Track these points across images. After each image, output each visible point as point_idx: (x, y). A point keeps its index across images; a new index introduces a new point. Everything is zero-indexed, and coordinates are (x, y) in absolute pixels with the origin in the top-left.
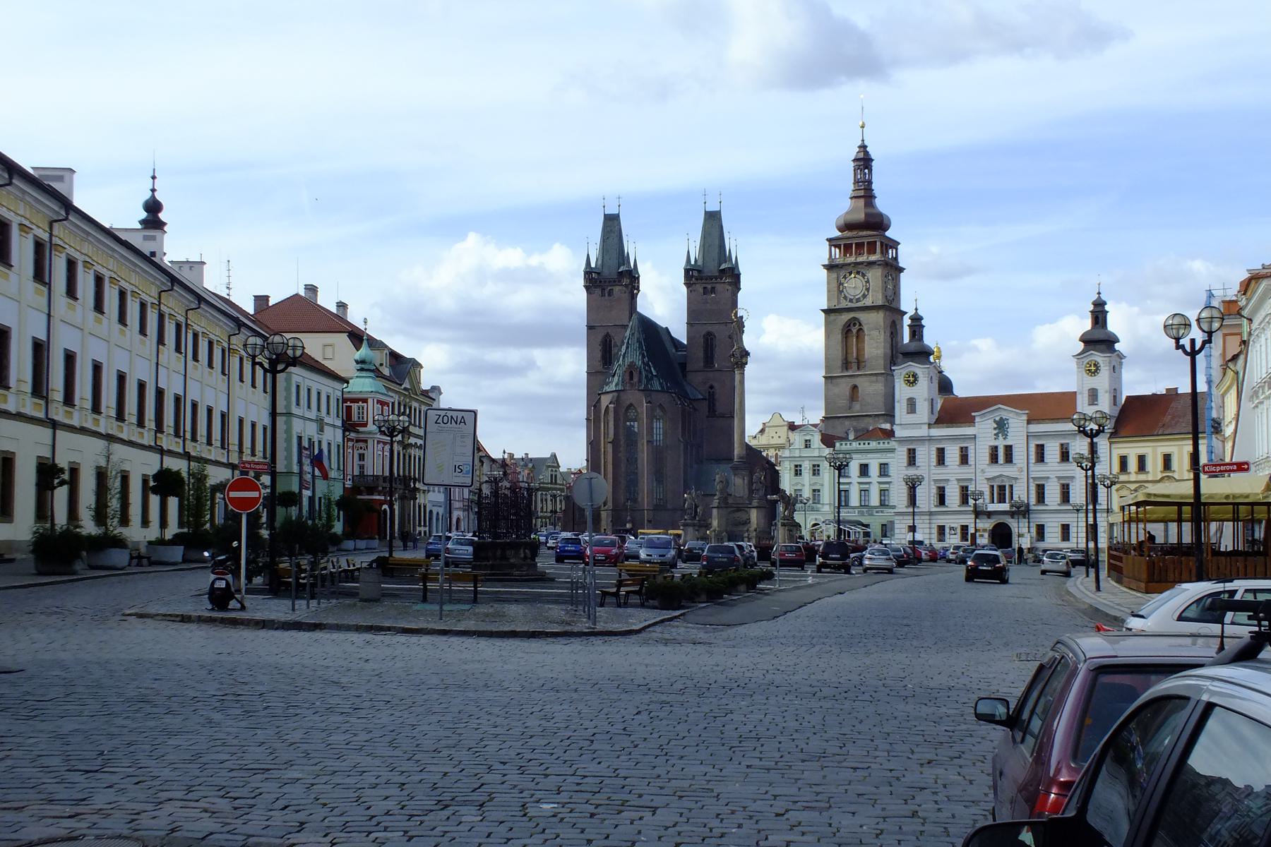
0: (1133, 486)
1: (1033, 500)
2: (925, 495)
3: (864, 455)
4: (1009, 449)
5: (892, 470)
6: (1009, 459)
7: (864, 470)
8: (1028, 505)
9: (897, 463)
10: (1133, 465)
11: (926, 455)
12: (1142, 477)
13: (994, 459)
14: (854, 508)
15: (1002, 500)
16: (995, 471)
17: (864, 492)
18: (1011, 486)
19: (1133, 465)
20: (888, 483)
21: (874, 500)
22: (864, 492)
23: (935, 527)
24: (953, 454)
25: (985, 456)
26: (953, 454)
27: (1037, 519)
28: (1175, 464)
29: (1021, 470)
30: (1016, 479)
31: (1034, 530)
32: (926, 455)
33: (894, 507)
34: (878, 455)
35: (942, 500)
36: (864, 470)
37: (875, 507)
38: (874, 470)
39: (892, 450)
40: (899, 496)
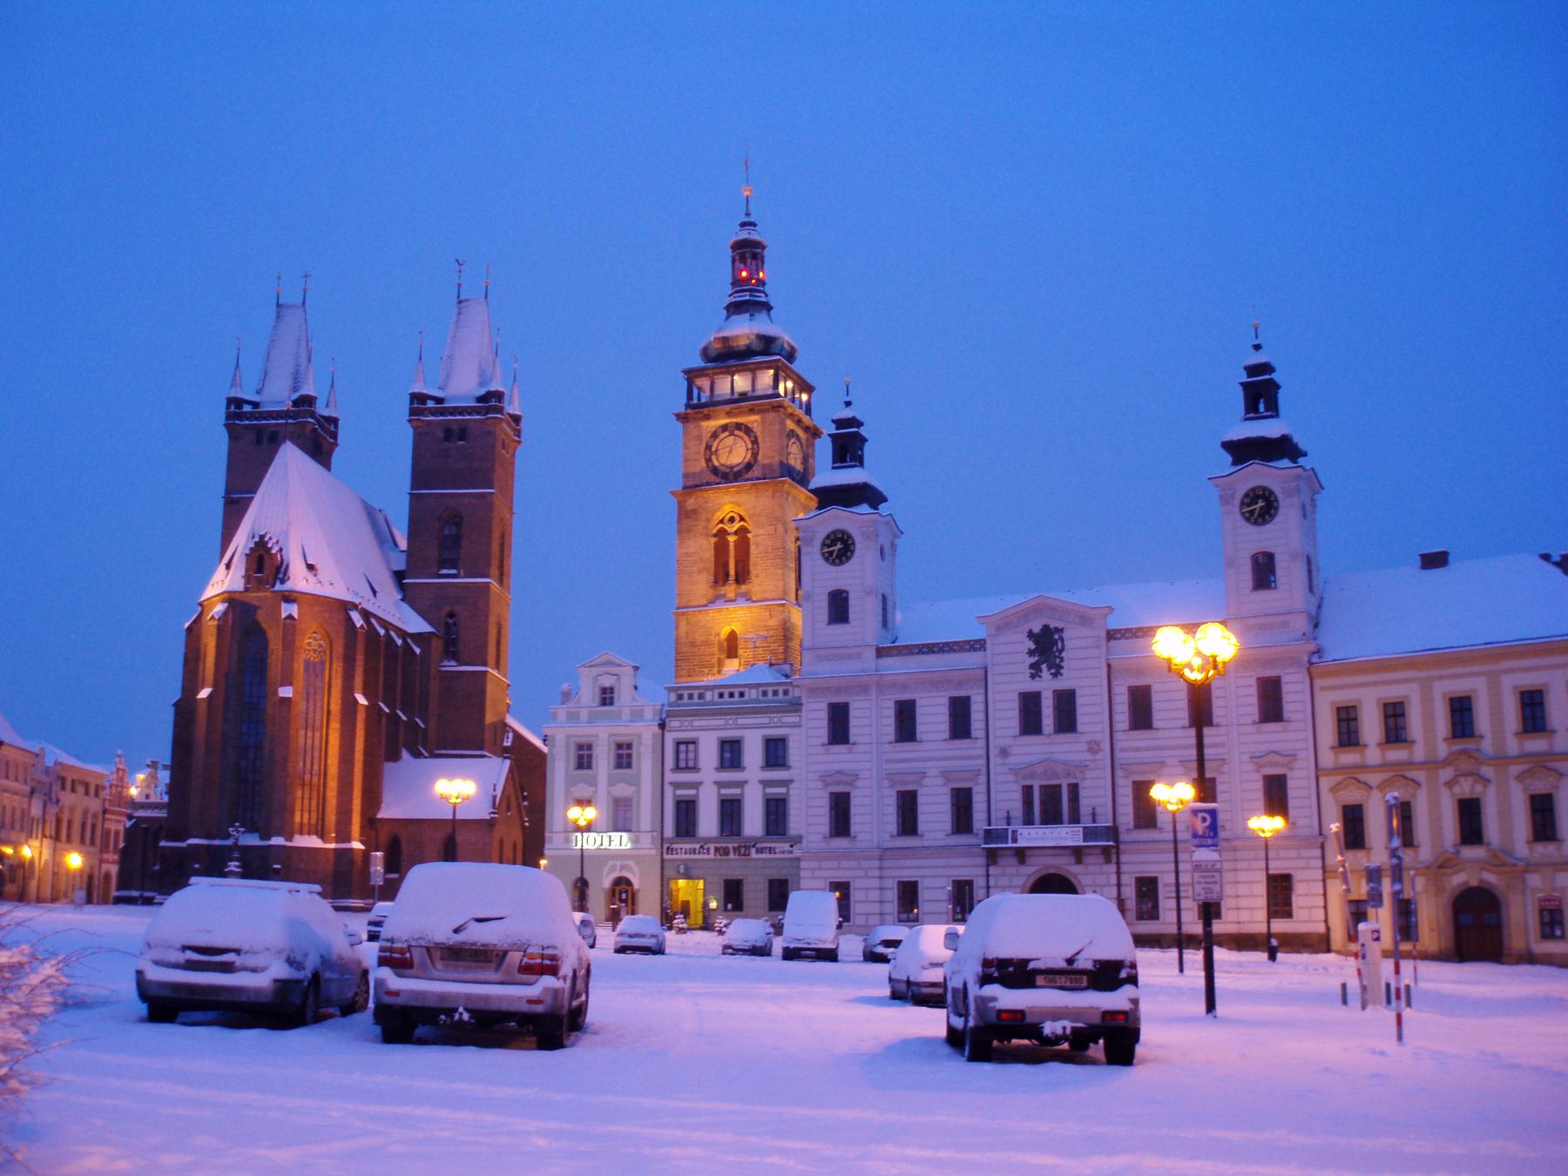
0: (1374, 779)
1: (1127, 817)
2: (873, 816)
3: (730, 720)
4: (1066, 704)
5: (794, 753)
6: (1067, 721)
7: (731, 754)
8: (1113, 832)
9: (806, 732)
10: (1371, 726)
11: (872, 720)
12: (1397, 754)
13: (1030, 722)
14: (708, 840)
15: (1052, 816)
16: (1031, 750)
17: (731, 811)
18: (1074, 789)
19: (1371, 726)
20: (786, 783)
21: (753, 822)
22: (731, 811)
23: (892, 884)
24: (933, 717)
25: (1006, 716)
26: (933, 717)
27: (1136, 864)
28: (1483, 718)
29: (1093, 748)
30: (1084, 767)
31: (1129, 892)
32: (872, 720)
33: (798, 840)
34: (764, 720)
35: (908, 820)
36: (731, 754)
37: (756, 840)
38: (753, 753)
39: (796, 706)
40: (808, 815)
